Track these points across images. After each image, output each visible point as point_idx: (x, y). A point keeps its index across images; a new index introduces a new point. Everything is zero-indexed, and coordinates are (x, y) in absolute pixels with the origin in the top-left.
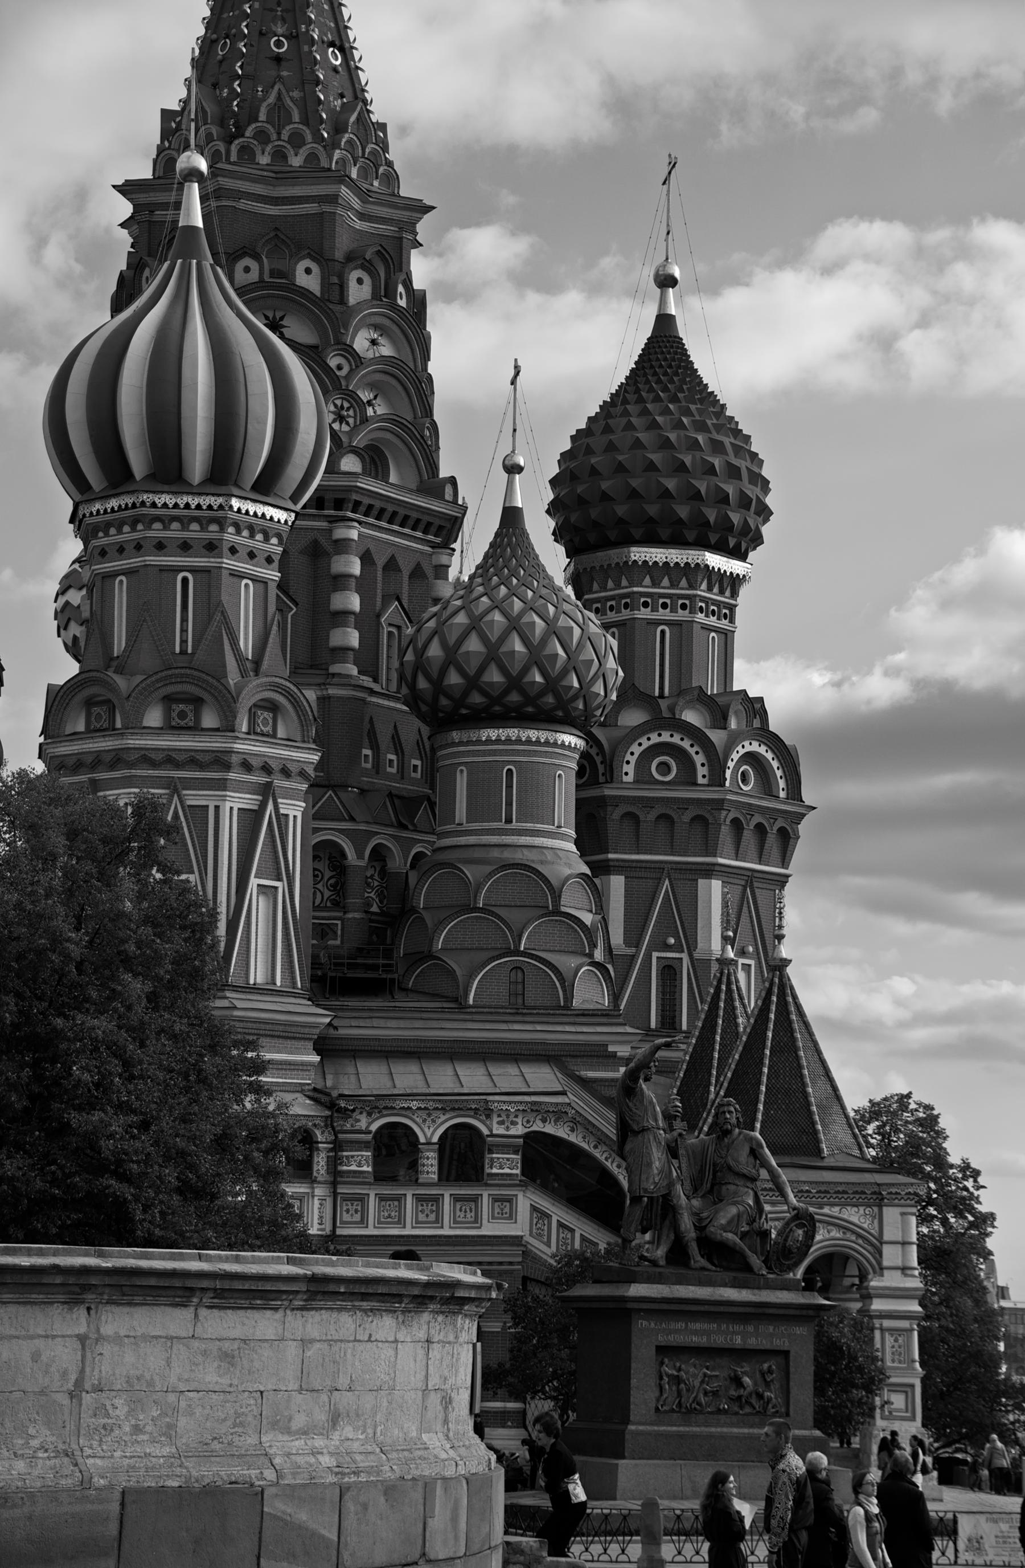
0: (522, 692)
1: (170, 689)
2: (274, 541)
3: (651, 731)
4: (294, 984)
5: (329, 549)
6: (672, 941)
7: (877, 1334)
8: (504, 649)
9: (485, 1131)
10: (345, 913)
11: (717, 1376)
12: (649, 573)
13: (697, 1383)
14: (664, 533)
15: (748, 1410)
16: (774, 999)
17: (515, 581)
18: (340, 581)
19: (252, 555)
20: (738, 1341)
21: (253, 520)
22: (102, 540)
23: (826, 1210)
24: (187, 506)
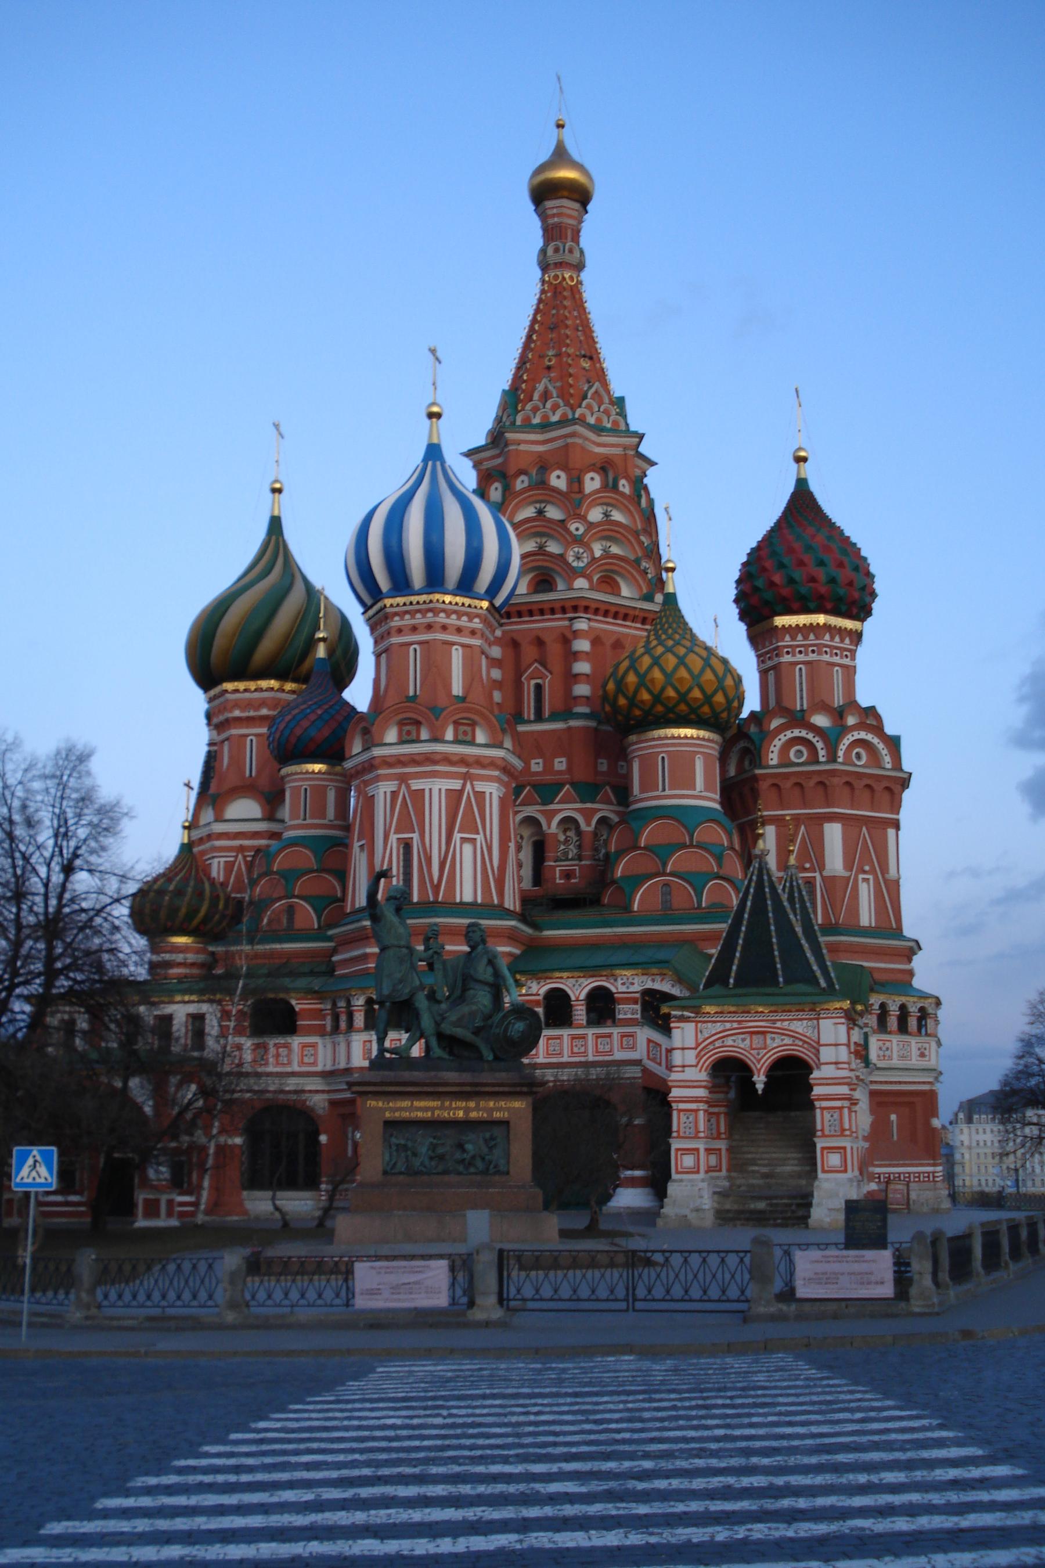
1: (401, 716)
2: (477, 620)
3: (787, 729)
5: (569, 636)
6: (807, 865)
7: (818, 1112)
8: (649, 677)
9: (614, 990)
10: (581, 860)
11: (443, 1144)
12: (788, 633)
13: (423, 1150)
14: (795, 606)
15: (472, 1170)
16: (754, 878)
17: (664, 637)
18: (576, 656)
19: (459, 630)
20: (461, 1114)
21: (456, 608)
22: (377, 633)
23: (778, 1024)
24: (411, 603)
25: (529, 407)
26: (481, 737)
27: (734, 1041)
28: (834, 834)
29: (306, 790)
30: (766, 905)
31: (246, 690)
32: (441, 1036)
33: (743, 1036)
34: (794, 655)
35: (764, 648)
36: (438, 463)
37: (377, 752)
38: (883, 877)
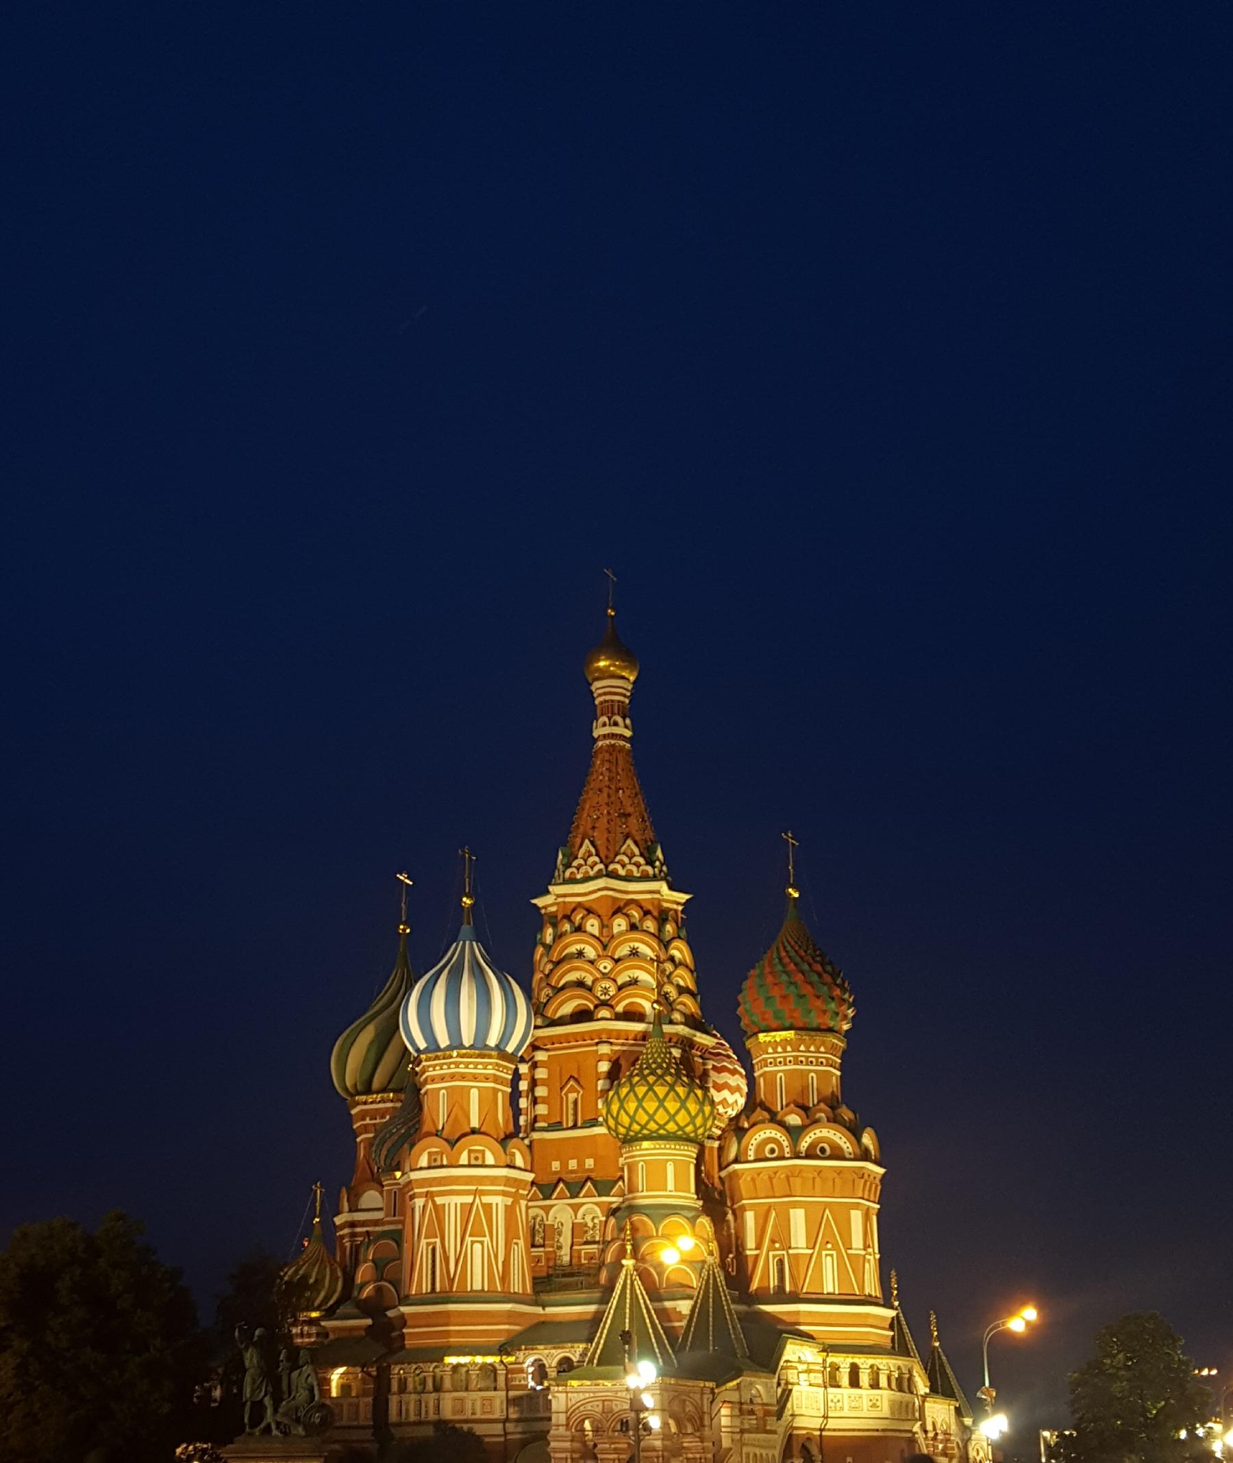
0: (638, 1124)
2: (490, 1067)
4: (497, 1288)
6: (777, 1245)
9: (575, 1359)
19: (475, 1078)
25: (575, 863)
26: (490, 1159)
27: (592, 1407)
28: (798, 1217)
29: (395, 1192)
30: (625, 1303)
31: (372, 1103)
32: (278, 1424)
33: (597, 1403)
34: (776, 1065)
35: (758, 1057)
36: (467, 942)
37: (414, 1176)
38: (846, 1252)
